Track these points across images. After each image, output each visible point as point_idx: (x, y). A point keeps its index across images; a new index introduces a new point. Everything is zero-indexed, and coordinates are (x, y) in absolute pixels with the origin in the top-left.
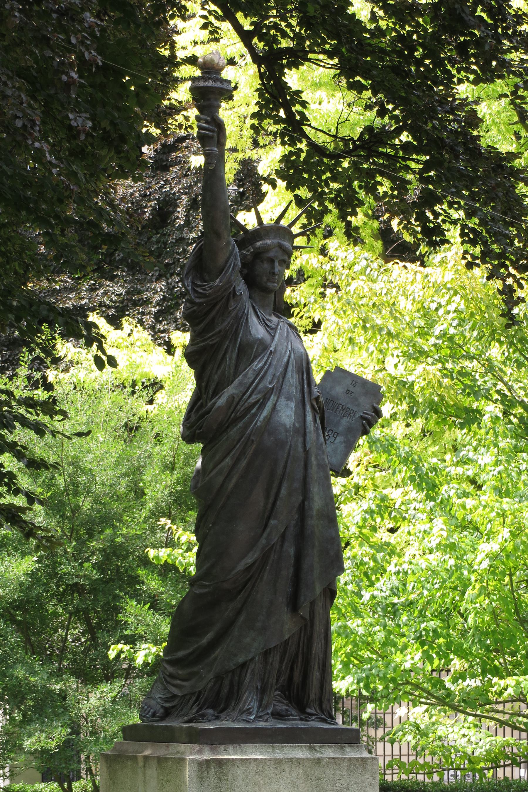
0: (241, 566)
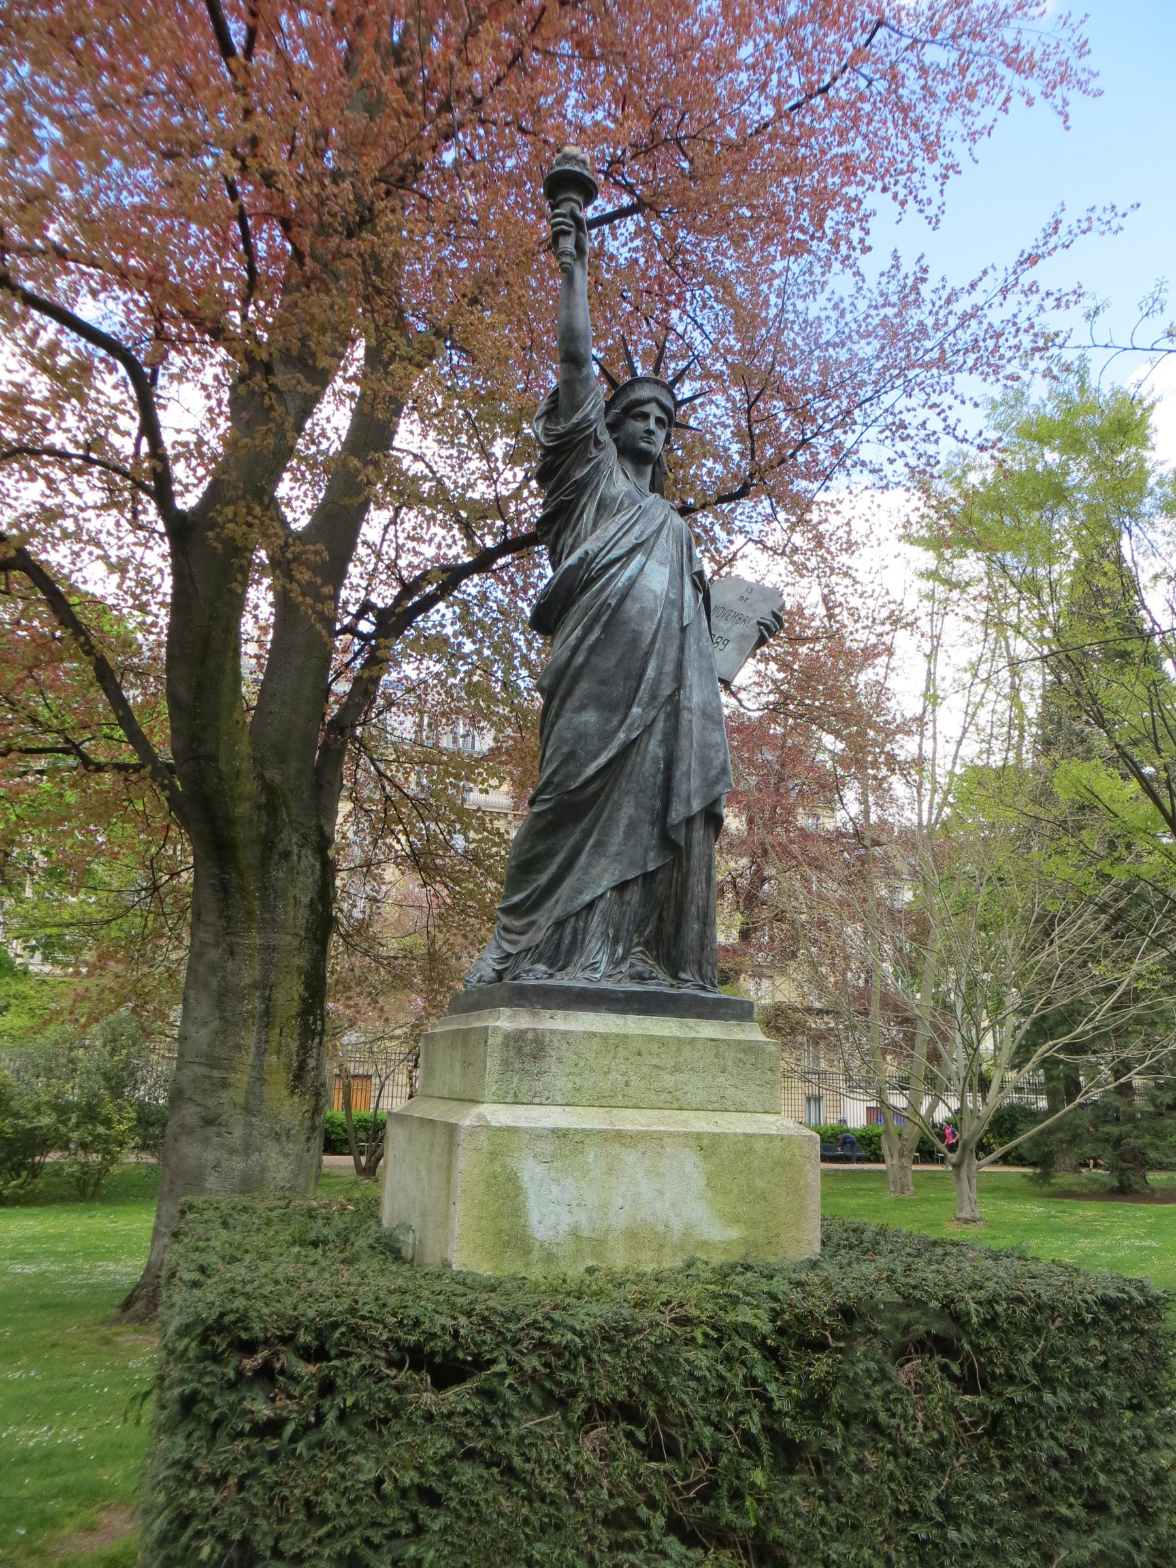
0: (591, 769)
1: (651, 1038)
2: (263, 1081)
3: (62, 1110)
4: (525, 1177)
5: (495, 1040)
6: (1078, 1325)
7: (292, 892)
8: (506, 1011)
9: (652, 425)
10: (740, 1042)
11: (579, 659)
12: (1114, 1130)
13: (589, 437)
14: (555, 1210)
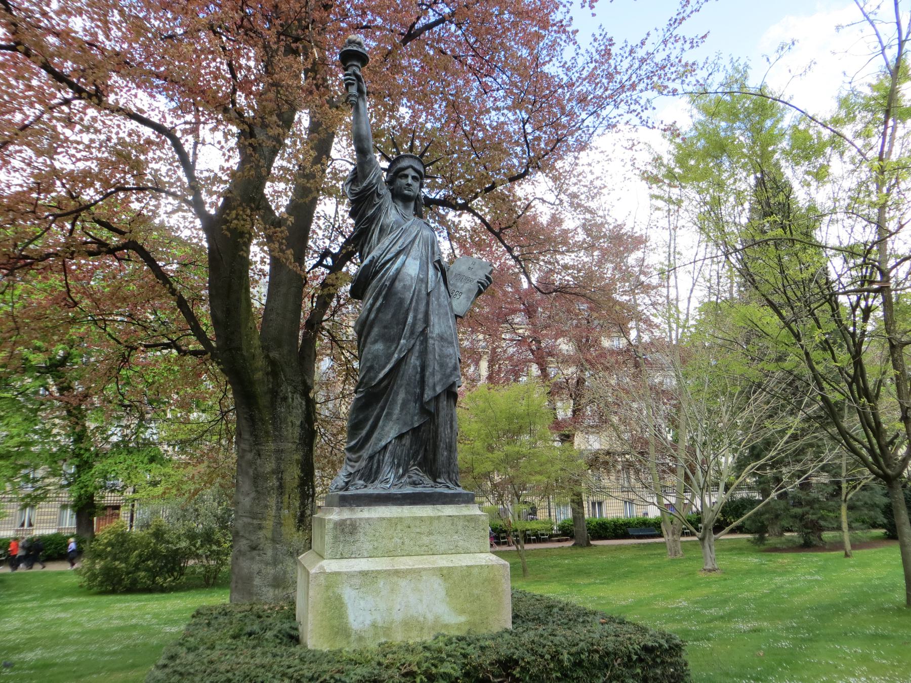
0: (381, 375)
1: (415, 518)
2: (281, 524)
3: (192, 536)
4: (346, 598)
5: (330, 526)
6: (629, 663)
7: (290, 419)
8: (336, 509)
9: (410, 181)
10: (465, 516)
11: (372, 316)
12: (798, 510)
13: (374, 192)
14: (362, 612)
